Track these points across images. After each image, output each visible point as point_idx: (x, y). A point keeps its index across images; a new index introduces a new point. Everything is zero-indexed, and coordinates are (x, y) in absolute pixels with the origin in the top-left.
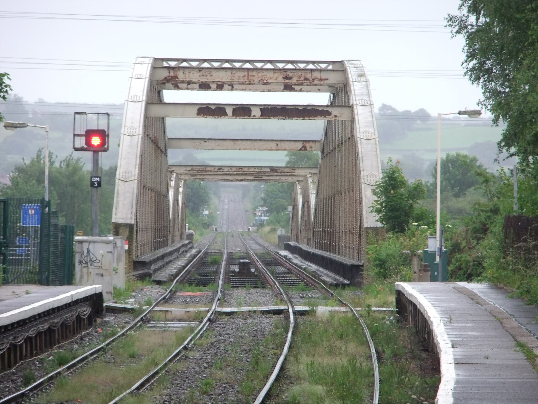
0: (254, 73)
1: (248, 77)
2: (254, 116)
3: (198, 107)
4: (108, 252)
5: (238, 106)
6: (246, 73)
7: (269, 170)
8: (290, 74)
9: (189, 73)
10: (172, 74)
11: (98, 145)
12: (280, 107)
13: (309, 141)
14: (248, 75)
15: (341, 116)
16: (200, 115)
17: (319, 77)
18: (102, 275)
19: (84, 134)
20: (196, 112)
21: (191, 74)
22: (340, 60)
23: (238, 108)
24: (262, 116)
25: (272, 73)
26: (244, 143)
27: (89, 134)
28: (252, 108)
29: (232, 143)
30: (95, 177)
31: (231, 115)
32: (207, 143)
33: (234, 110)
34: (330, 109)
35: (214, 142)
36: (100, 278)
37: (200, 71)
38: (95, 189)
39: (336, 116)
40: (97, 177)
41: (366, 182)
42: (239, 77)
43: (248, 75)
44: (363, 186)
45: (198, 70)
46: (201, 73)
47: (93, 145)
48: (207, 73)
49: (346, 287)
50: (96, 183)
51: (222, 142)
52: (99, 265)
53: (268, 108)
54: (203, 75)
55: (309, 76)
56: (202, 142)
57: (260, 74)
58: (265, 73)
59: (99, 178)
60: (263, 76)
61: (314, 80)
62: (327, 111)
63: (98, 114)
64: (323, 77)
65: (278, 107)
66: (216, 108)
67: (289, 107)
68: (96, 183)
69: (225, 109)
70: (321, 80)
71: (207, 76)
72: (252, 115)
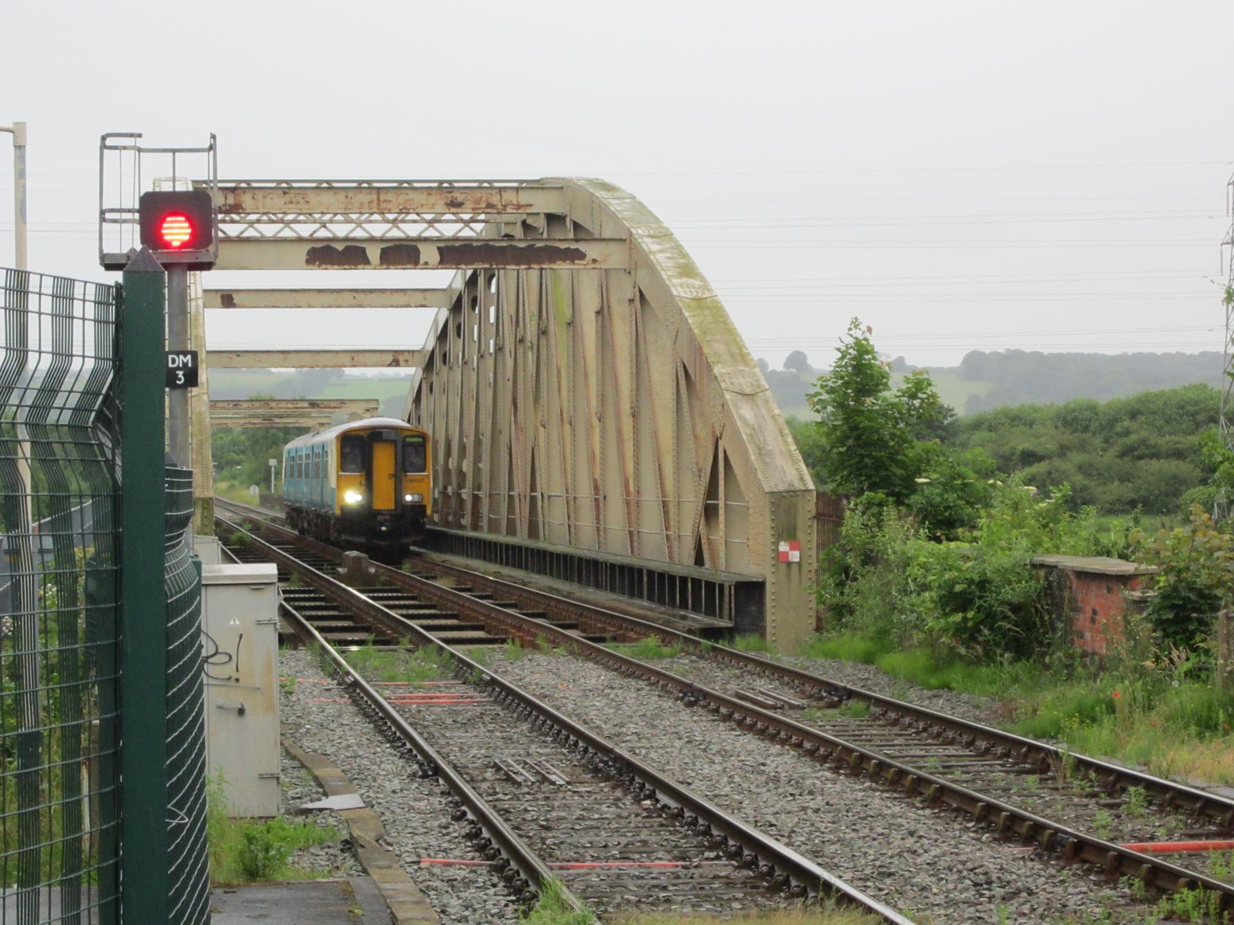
0: (390, 196)
1: (378, 204)
2: (426, 263)
3: (309, 246)
4: (259, 623)
5: (391, 244)
6: (374, 197)
7: (306, 405)
8: (460, 197)
9: (265, 197)
10: (231, 201)
11: (184, 245)
12: (479, 244)
13: (403, 352)
14: (379, 200)
15: (605, 261)
16: (314, 263)
17: (515, 202)
18: (241, 712)
19: (137, 206)
20: (304, 257)
21: (268, 201)
22: (537, 178)
23: (395, 246)
24: (441, 262)
25: (425, 195)
26: (301, 356)
27: (154, 209)
28: (422, 247)
29: (281, 356)
30: (178, 353)
31: (378, 261)
32: (241, 359)
33: (384, 252)
34: (582, 247)
35: (251, 356)
36: (234, 720)
37: (285, 193)
38: (177, 392)
39: (594, 261)
40: (185, 354)
41: (732, 388)
42: (362, 203)
43: (379, 200)
44: (728, 396)
45: (280, 192)
46: (287, 198)
47: (167, 245)
48: (299, 198)
49: (738, 638)
50: (180, 374)
51: (266, 355)
52: (229, 670)
53: (453, 247)
54: (291, 202)
55: (495, 200)
56: (234, 356)
57: (402, 199)
58: (412, 195)
59: (189, 357)
60: (406, 201)
61: (505, 207)
62: (577, 250)
63: (174, 151)
64: (523, 202)
65: (475, 244)
66: (347, 248)
67: (497, 244)
68: (180, 374)
69: (364, 250)
70: (519, 207)
71: (298, 203)
72: (422, 261)
